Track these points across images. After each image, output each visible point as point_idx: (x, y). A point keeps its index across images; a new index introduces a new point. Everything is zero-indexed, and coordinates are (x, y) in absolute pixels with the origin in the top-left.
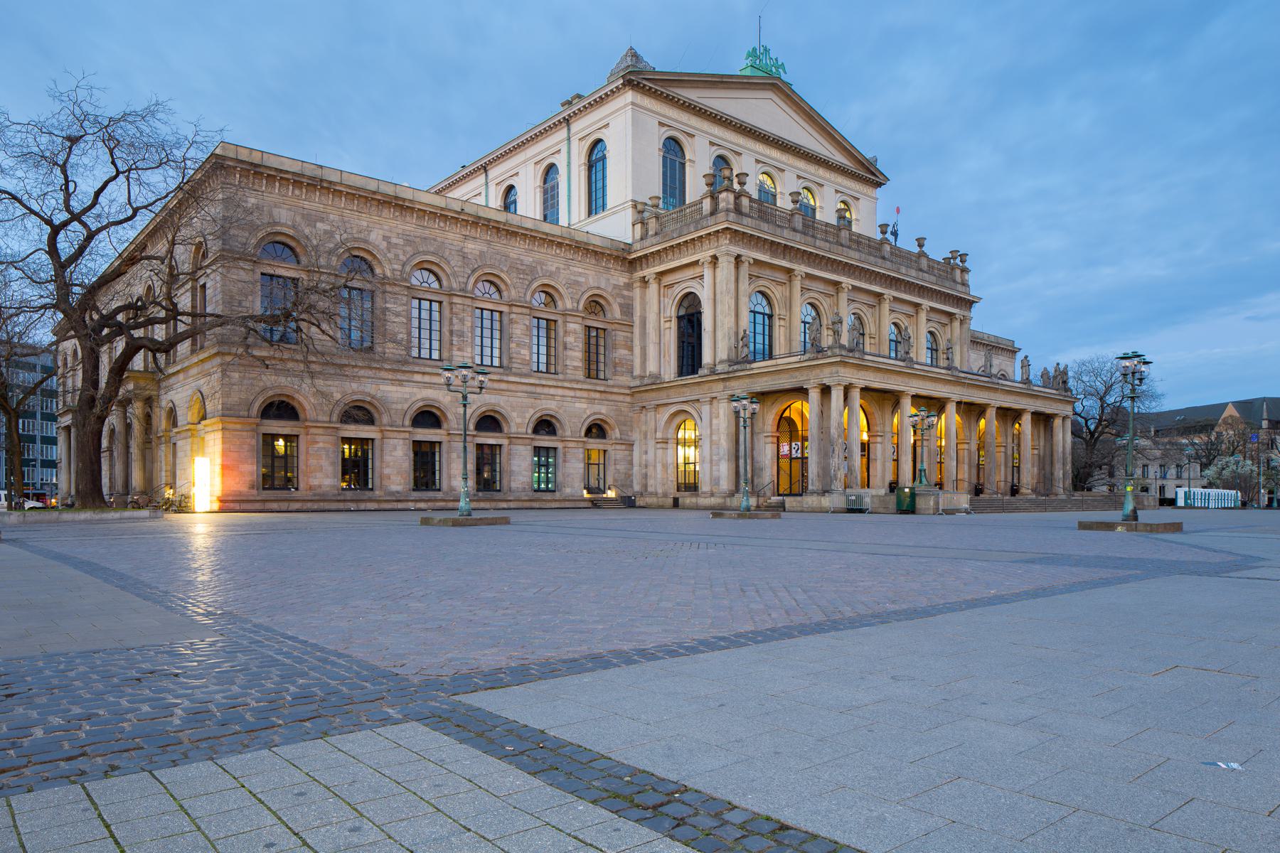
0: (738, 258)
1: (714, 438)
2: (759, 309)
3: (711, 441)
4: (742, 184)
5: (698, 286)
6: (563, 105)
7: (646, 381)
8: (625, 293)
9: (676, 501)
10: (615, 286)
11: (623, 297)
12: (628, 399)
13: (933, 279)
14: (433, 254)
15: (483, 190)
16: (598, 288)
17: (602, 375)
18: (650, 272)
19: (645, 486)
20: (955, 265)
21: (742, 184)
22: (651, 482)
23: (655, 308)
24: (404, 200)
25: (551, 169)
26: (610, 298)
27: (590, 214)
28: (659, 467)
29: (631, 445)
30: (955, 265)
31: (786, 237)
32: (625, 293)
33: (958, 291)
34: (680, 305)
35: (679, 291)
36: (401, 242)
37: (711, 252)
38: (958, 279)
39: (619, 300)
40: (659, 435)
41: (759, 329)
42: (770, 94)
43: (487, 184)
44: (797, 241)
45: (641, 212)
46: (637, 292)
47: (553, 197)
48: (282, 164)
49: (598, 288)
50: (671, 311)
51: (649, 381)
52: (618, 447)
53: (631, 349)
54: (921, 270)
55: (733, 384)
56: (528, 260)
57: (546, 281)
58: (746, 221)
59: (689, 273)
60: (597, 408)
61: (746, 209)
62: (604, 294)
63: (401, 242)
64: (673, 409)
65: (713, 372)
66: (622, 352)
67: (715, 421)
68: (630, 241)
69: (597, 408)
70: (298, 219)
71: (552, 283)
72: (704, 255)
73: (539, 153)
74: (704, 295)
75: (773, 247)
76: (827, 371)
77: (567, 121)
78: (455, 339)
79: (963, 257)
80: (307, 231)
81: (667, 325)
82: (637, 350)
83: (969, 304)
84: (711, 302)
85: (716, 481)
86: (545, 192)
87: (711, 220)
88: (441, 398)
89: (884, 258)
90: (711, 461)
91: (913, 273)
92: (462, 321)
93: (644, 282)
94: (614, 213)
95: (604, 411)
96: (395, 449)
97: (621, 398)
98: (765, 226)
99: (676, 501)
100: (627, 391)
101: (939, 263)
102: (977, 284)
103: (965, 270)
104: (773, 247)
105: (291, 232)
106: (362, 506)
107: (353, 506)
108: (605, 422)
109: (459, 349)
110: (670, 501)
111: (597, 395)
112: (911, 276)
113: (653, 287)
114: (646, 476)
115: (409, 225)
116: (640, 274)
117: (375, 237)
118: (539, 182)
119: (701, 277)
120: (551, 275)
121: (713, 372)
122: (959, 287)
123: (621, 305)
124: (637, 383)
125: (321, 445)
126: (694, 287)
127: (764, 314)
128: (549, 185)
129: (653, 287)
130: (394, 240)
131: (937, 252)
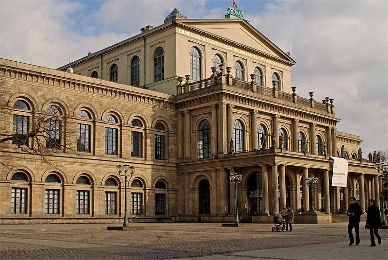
0: (228, 105)
1: (218, 188)
2: (237, 127)
3: (217, 190)
4: (228, 72)
5: (209, 117)
6: (142, 30)
7: (184, 160)
8: (174, 119)
9: (199, 218)
10: (169, 116)
11: (173, 120)
12: (175, 169)
13: (318, 111)
14: (87, 104)
15: (100, 65)
16: (161, 117)
17: (162, 157)
18: (185, 109)
19: (184, 211)
20: (327, 104)
21: (228, 72)
22: (187, 209)
23: (188, 126)
24: (76, 80)
25: (135, 59)
26: (167, 122)
27: (155, 81)
28: (191, 202)
29: (176, 191)
30: (327, 104)
31: (248, 94)
32: (174, 119)
33: (330, 116)
34: (200, 125)
35: (199, 119)
36: (74, 99)
37: (215, 102)
38: (329, 110)
39: (170, 122)
40: (191, 186)
41: (238, 136)
42: (239, 26)
43: (102, 62)
44: (254, 96)
45: (181, 81)
46: (180, 118)
47: (136, 71)
48: (24, 66)
49: (161, 117)
50: (196, 127)
51: (186, 161)
52: (170, 192)
53: (177, 145)
54: (312, 107)
55: (226, 163)
56: (129, 105)
57: (138, 115)
58: (231, 88)
59: (204, 111)
60: (161, 174)
61: (231, 83)
62: (164, 120)
63: (74, 99)
64: (198, 174)
65: (217, 157)
66: (172, 147)
67: (218, 180)
68: (175, 95)
69: (161, 174)
70: (30, 90)
71: (140, 115)
72: (212, 103)
73: (130, 51)
74: (212, 121)
75: (243, 100)
76: (270, 158)
77: (144, 38)
78: (96, 142)
79: (331, 100)
80: (34, 95)
81: (194, 134)
82: (180, 146)
83: (335, 122)
84: (215, 125)
85: (218, 209)
86: (132, 68)
87: (215, 88)
88: (90, 171)
89: (294, 102)
90: (217, 199)
91: (308, 109)
92: (100, 134)
93: (183, 114)
94: (168, 81)
95: (164, 175)
96: (69, 194)
97: (172, 168)
98: (240, 91)
99: (199, 218)
100: (175, 165)
101: (320, 104)
102: (337, 113)
103: (332, 106)
104: (243, 100)
105: (27, 96)
106: (55, 221)
107: (50, 221)
108: (164, 180)
109: (98, 147)
110: (197, 219)
111: (161, 167)
112: (307, 109)
113: (187, 116)
114: (184, 206)
115: (77, 91)
116: (181, 110)
117: (63, 96)
118: (129, 64)
119: (211, 113)
120: (140, 112)
121: (217, 157)
122: (330, 115)
123: (172, 124)
124: (180, 161)
125: (37, 192)
126: (207, 118)
127: (239, 130)
128: (134, 65)
129: (187, 116)
130: (71, 98)
131: (318, 98)
